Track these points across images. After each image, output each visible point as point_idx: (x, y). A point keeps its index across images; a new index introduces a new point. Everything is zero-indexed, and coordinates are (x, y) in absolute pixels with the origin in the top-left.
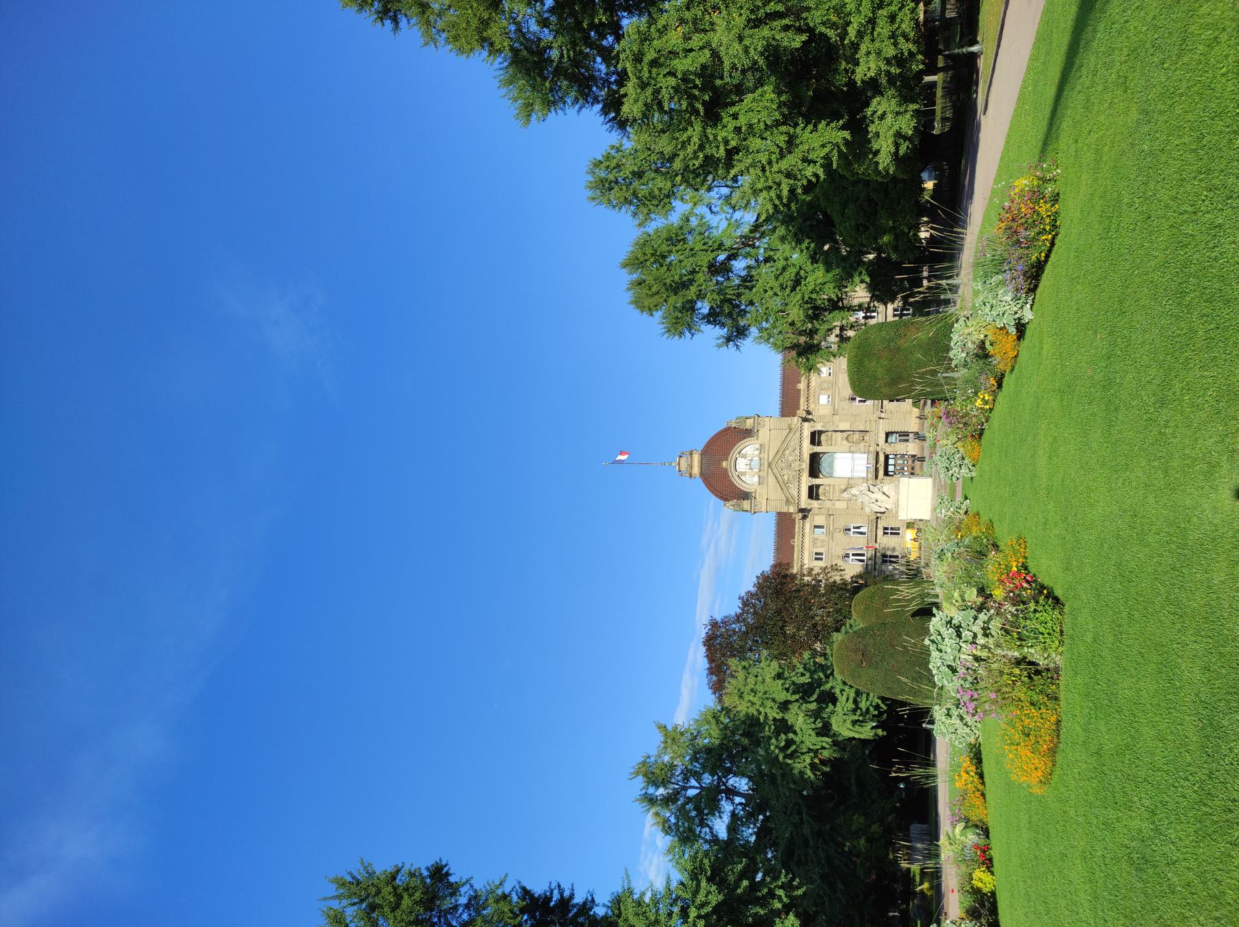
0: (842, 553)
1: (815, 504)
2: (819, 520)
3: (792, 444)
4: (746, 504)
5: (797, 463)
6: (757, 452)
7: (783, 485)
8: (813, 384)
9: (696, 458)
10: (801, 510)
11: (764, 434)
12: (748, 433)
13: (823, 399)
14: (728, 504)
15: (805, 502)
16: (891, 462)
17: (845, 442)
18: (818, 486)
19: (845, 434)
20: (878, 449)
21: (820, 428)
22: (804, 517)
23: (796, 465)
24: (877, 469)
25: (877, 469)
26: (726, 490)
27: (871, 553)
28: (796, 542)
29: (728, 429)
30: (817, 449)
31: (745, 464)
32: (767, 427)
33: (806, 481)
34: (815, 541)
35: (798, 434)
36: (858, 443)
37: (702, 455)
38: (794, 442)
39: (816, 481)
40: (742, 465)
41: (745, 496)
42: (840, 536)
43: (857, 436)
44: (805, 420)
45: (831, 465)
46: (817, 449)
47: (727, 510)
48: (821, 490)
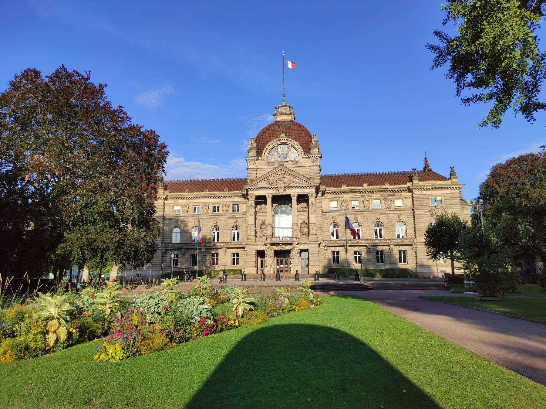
0: (219, 224)
1: (252, 201)
2: (243, 208)
3: (298, 181)
4: (253, 154)
5: (283, 186)
6: (293, 159)
8: (346, 196)
9: (289, 118)
11: (308, 162)
12: (307, 151)
13: (334, 204)
17: (301, 221)
18: (265, 203)
19: (307, 221)
21: (311, 200)
23: (281, 184)
24: (278, 244)
25: (278, 244)
27: (218, 245)
28: (227, 193)
29: (310, 136)
30: (294, 201)
34: (227, 205)
35: (305, 184)
36: (301, 230)
37: (291, 121)
39: (269, 201)
40: (281, 148)
41: (259, 153)
42: (232, 222)
43: (306, 230)
44: (317, 191)
45: (284, 213)
46: (294, 201)
47: (249, 143)
48: (263, 206)
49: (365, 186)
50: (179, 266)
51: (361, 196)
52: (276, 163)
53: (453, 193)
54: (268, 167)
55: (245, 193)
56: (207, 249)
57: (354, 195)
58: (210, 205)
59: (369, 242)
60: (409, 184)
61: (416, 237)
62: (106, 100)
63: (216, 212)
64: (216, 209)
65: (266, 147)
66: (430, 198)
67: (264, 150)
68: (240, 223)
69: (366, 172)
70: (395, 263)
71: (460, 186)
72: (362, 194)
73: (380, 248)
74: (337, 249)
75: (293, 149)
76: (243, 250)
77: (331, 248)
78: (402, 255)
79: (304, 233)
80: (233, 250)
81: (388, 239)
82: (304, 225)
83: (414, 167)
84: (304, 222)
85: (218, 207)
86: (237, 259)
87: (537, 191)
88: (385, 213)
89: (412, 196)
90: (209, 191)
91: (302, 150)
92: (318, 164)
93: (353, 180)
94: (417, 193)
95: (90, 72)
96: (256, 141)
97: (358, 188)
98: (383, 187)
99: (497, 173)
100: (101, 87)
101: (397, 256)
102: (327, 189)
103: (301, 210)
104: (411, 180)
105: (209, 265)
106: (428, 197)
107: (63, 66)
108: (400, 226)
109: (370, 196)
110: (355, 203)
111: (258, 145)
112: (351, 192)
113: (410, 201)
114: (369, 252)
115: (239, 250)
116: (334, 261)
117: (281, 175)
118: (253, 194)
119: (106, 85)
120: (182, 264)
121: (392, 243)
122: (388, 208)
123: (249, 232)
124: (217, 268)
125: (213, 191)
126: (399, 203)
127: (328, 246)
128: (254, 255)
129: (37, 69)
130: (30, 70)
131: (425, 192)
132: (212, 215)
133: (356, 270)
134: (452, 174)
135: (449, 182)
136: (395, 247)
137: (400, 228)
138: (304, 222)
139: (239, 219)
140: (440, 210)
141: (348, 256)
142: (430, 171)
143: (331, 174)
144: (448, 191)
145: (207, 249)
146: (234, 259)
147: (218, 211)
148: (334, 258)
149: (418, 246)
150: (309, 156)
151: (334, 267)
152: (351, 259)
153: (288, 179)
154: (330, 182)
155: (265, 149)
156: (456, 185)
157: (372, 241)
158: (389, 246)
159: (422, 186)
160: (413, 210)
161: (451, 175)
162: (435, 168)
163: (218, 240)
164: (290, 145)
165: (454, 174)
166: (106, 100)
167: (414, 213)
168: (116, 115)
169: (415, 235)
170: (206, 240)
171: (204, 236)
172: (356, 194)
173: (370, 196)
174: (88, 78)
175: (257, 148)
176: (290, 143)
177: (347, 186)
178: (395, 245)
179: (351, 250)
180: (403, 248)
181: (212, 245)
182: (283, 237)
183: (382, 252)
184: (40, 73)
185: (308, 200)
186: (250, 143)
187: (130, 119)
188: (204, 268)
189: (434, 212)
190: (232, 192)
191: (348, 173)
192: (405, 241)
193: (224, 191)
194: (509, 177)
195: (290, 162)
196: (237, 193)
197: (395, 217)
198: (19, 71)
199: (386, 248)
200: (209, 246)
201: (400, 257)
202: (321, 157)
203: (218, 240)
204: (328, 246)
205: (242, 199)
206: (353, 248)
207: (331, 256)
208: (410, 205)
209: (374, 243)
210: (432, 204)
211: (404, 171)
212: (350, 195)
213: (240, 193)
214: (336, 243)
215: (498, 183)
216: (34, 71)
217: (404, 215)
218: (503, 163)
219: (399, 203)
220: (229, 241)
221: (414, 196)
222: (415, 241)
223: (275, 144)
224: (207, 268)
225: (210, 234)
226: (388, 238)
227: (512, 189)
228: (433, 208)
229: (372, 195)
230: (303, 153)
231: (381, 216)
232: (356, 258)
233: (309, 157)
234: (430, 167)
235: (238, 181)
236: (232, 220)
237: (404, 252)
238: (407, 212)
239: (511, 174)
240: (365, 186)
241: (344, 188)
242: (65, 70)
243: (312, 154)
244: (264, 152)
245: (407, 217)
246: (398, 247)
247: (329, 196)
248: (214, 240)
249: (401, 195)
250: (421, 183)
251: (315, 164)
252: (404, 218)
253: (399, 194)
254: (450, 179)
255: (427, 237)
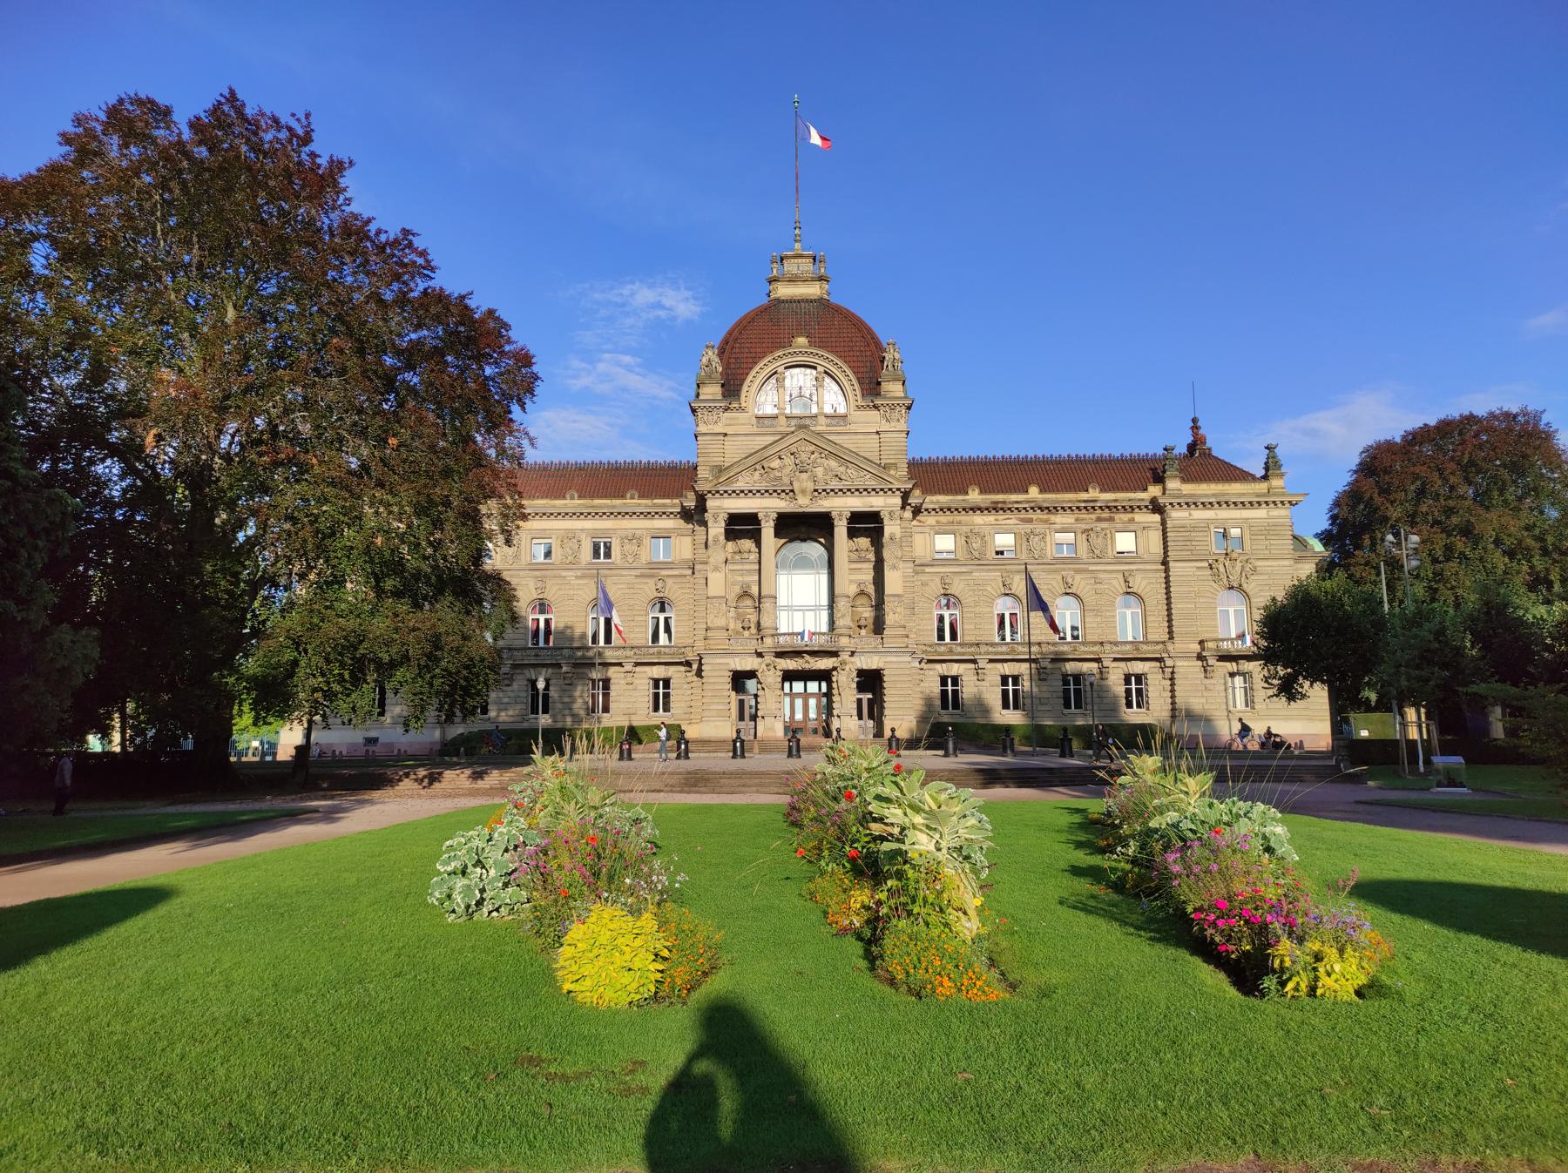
1: (717, 529)
4: (712, 391)
5: (810, 486)
6: (828, 410)
7: (758, 461)
8: (978, 519)
9: (813, 290)
10: (701, 506)
12: (871, 387)
13: (945, 543)
14: (712, 355)
15: (721, 507)
16: (813, 687)
18: (756, 536)
19: (871, 589)
20: (844, 656)
21: (887, 531)
22: (686, 515)
23: (804, 482)
24: (797, 654)
25: (797, 654)
26: (740, 354)
28: (633, 502)
29: (880, 348)
31: (800, 389)
32: (885, 426)
33: (768, 507)
34: (635, 539)
35: (873, 483)
37: (821, 302)
38: (854, 477)
40: (799, 379)
41: (732, 389)
42: (649, 590)
43: (867, 613)
49: (1034, 492)
50: (492, 714)
51: (1022, 520)
52: (782, 420)
53: (1279, 517)
54: (756, 430)
55: (691, 503)
56: (576, 665)
57: (1001, 516)
58: (583, 537)
59: (1045, 649)
60: (1154, 490)
61: (1171, 638)
62: (347, 209)
63: (602, 559)
64: (601, 550)
65: (753, 373)
66: (1213, 530)
67: (747, 382)
68: (673, 591)
69: (1031, 455)
70: (1114, 709)
71: (1294, 499)
72: (1023, 515)
73: (1070, 667)
74: (955, 669)
75: (828, 380)
76: (682, 669)
77: (938, 666)
78: (1134, 687)
79: (863, 622)
80: (655, 668)
81: (1095, 643)
82: (863, 600)
83: (1170, 444)
84: (862, 593)
85: (608, 548)
86: (666, 696)
87: (1493, 515)
88: (1087, 571)
89: (1163, 523)
90: (580, 497)
91: (857, 386)
92: (902, 426)
93: (1001, 476)
94: (1176, 515)
95: (307, 116)
96: (721, 353)
97: (1014, 497)
98: (1084, 496)
99: (1376, 464)
100: (338, 167)
101: (1120, 690)
102: (928, 498)
103: (854, 556)
104: (1159, 479)
105: (582, 713)
106: (1207, 524)
107: (232, 97)
108: (1128, 606)
109: (1046, 521)
110: (1005, 540)
111: (727, 366)
112: (995, 508)
113: (1155, 537)
114: (1041, 675)
115: (672, 669)
116: (944, 705)
117: (804, 456)
118: (719, 508)
119: (351, 163)
120: (500, 710)
121: (1108, 654)
122: (1097, 556)
123: (710, 617)
124: (608, 721)
125: (592, 497)
126: (1125, 542)
127: (930, 661)
128: (726, 683)
129: (162, 100)
130: (139, 102)
131: (1200, 514)
132: (589, 566)
133: (1008, 729)
134: (1272, 467)
135: (1263, 486)
136: (1115, 664)
137: (1129, 612)
138: (862, 593)
139: (670, 582)
140: (1239, 565)
141: (982, 688)
142: (1207, 454)
143: (934, 457)
144: (1261, 513)
145: (576, 665)
146: (656, 696)
147: (608, 555)
148: (944, 693)
149: (1179, 663)
150: (878, 402)
151: (946, 719)
152: (993, 698)
153: (824, 469)
154: (935, 477)
155: (750, 378)
156: (1283, 494)
157: (1052, 649)
158: (1098, 660)
159: (1191, 496)
160: (1165, 563)
161: (1267, 469)
162: (1220, 446)
163: (608, 640)
164: (820, 369)
165: (1278, 465)
166: (347, 209)
167: (1167, 571)
168: (398, 257)
169: (1170, 632)
170: (572, 639)
171: (567, 627)
172: (1008, 515)
173: (1046, 521)
174: (307, 139)
175: (725, 374)
176: (823, 364)
177: (981, 492)
178: (1116, 660)
179: (994, 672)
180: (1138, 667)
181: (591, 653)
182: (812, 634)
183: (1078, 678)
184: (167, 112)
185: (882, 528)
186: (704, 360)
187: (433, 270)
188: (569, 720)
189: (1222, 569)
190: (648, 502)
191: (982, 455)
192: (1145, 647)
193: (623, 497)
194: (1416, 477)
195: (822, 420)
196: (664, 505)
197: (1115, 582)
198: (95, 104)
199: (1086, 667)
200: (584, 657)
201: (1128, 692)
202: (909, 408)
203: (608, 640)
204: (930, 661)
205: (681, 523)
206: (999, 665)
207: (936, 689)
208: (1156, 547)
209: (1056, 653)
210: (1216, 549)
211: (1135, 453)
212: (990, 518)
213: (673, 504)
214: (951, 652)
215: (1385, 491)
216: (149, 105)
217: (1139, 577)
218: (1398, 440)
219: (1125, 542)
220: (643, 642)
221: (1169, 524)
222: (1170, 647)
223: (778, 366)
224: (577, 719)
225: (585, 624)
226: (1095, 638)
227: (1424, 509)
228: (1221, 559)
229: (1053, 518)
230: (858, 392)
231: (1078, 577)
232: (1005, 694)
233: (876, 407)
234: (1208, 444)
235: (662, 468)
236: (651, 581)
237: (1139, 678)
238: (1148, 567)
239: (1421, 470)
240: (1034, 492)
241: (974, 496)
242: (240, 111)
243: (885, 398)
244: (745, 388)
245: (1148, 583)
246: (1122, 664)
247: (930, 520)
248: (595, 639)
249: (1132, 520)
250: (1188, 488)
251: (894, 426)
252: (1138, 584)
253: (1126, 517)
254: (1265, 477)
255: (1261, 634)
